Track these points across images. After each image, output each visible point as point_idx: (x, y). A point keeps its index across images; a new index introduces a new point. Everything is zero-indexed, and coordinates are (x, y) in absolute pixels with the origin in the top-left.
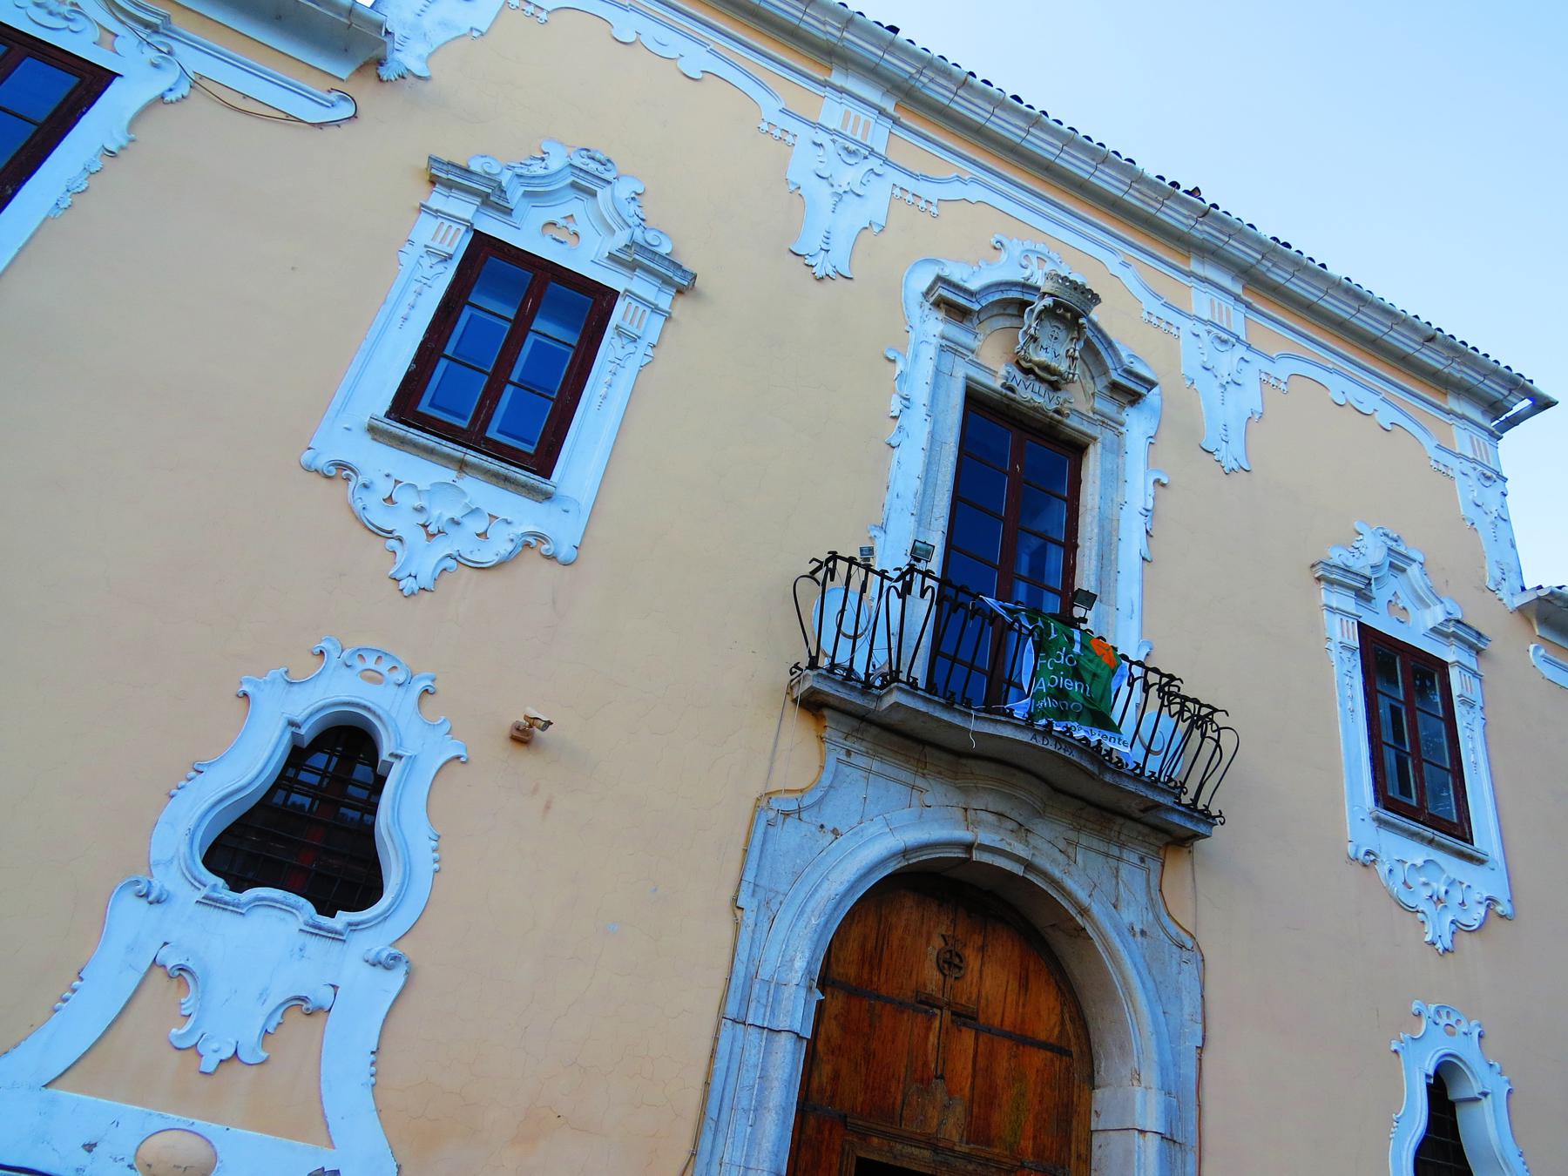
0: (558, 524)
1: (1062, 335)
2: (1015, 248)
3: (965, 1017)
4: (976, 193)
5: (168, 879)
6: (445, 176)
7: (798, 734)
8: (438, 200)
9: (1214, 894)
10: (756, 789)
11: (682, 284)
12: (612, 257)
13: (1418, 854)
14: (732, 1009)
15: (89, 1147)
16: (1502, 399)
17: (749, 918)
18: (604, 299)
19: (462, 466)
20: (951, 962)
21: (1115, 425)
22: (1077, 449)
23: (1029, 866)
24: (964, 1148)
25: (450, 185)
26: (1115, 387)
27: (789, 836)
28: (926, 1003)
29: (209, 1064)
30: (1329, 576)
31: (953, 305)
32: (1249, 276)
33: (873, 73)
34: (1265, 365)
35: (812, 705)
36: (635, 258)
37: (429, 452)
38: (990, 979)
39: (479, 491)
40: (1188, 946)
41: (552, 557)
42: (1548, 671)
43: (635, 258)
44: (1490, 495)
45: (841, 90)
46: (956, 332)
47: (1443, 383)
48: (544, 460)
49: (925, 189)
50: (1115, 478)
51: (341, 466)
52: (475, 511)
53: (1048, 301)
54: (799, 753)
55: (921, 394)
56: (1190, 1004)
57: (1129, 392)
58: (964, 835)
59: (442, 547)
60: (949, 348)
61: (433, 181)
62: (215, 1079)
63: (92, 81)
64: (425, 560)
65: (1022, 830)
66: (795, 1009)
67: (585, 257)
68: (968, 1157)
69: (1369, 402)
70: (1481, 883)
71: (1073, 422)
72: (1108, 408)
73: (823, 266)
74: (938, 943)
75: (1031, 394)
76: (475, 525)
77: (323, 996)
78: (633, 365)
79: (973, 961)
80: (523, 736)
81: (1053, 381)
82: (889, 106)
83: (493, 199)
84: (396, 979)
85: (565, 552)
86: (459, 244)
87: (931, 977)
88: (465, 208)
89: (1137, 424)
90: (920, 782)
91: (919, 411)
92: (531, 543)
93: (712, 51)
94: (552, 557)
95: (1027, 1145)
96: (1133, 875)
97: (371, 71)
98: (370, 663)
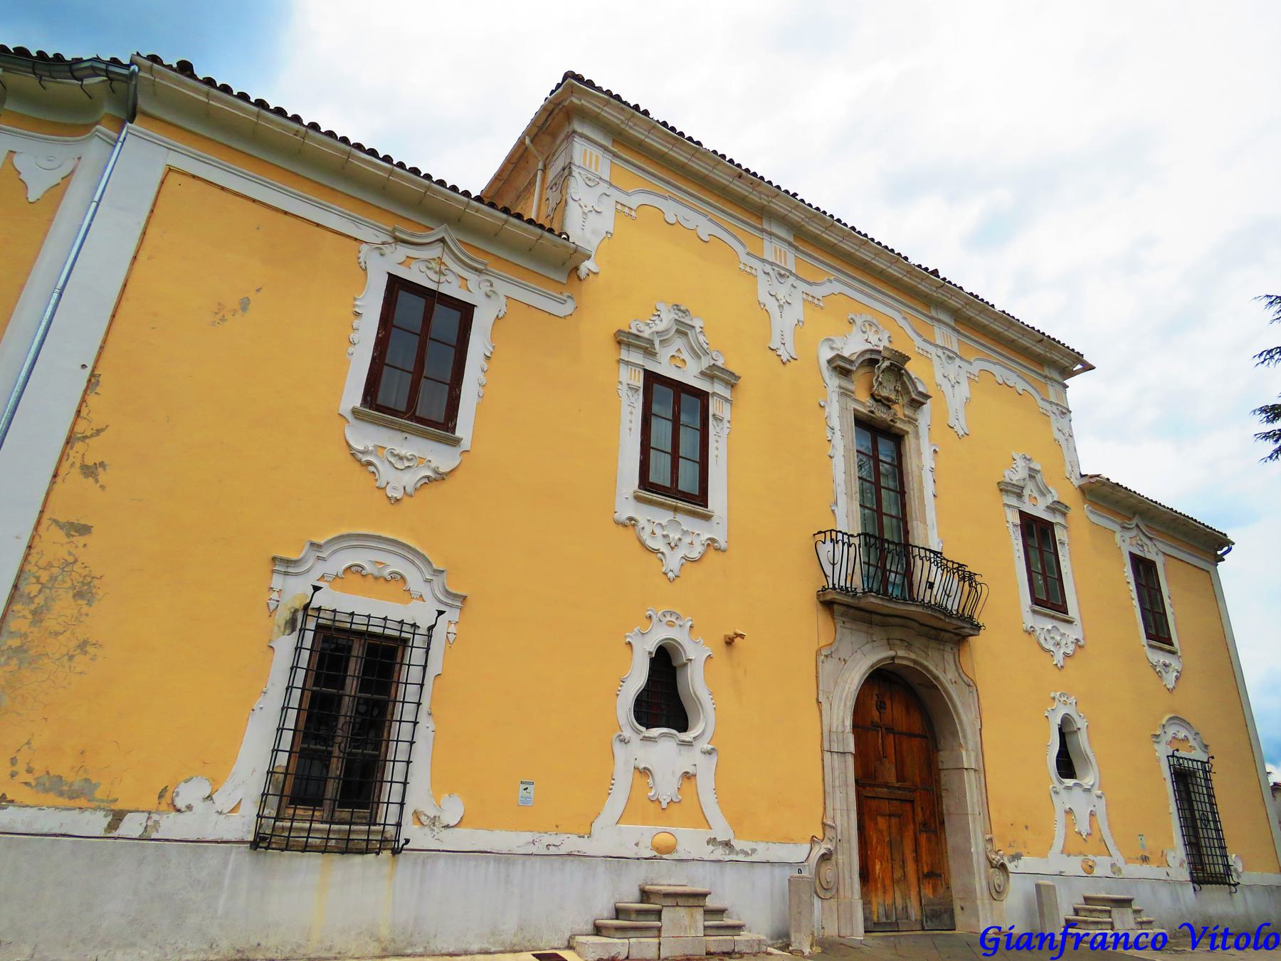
0: (717, 530)
1: (892, 379)
3: (890, 730)
5: (627, 733)
6: (625, 340)
8: (624, 355)
10: (816, 648)
12: (702, 373)
14: (826, 747)
15: (637, 845)
17: (825, 706)
18: (703, 396)
19: (676, 509)
21: (912, 421)
23: (915, 662)
24: (897, 785)
25: (629, 345)
26: (913, 400)
29: (664, 805)
30: (1006, 488)
31: (841, 368)
32: (957, 315)
33: (783, 221)
36: (712, 373)
37: (661, 505)
41: (717, 549)
42: (1094, 518)
43: (712, 373)
44: (1062, 423)
45: (771, 234)
46: (845, 383)
51: (631, 519)
52: (685, 532)
53: (887, 363)
58: (892, 653)
59: (681, 552)
61: (619, 343)
62: (662, 810)
63: (466, 311)
64: (673, 561)
65: (909, 647)
67: (689, 375)
68: (899, 788)
69: (1013, 379)
70: (1073, 633)
71: (899, 425)
72: (908, 412)
74: (875, 698)
75: (881, 414)
76: (687, 540)
77: (691, 770)
78: (724, 436)
81: (886, 403)
84: (714, 759)
85: (723, 545)
86: (639, 382)
88: (637, 357)
90: (871, 631)
93: (710, 220)
94: (717, 549)
95: (918, 779)
97: (574, 275)
98: (669, 618)
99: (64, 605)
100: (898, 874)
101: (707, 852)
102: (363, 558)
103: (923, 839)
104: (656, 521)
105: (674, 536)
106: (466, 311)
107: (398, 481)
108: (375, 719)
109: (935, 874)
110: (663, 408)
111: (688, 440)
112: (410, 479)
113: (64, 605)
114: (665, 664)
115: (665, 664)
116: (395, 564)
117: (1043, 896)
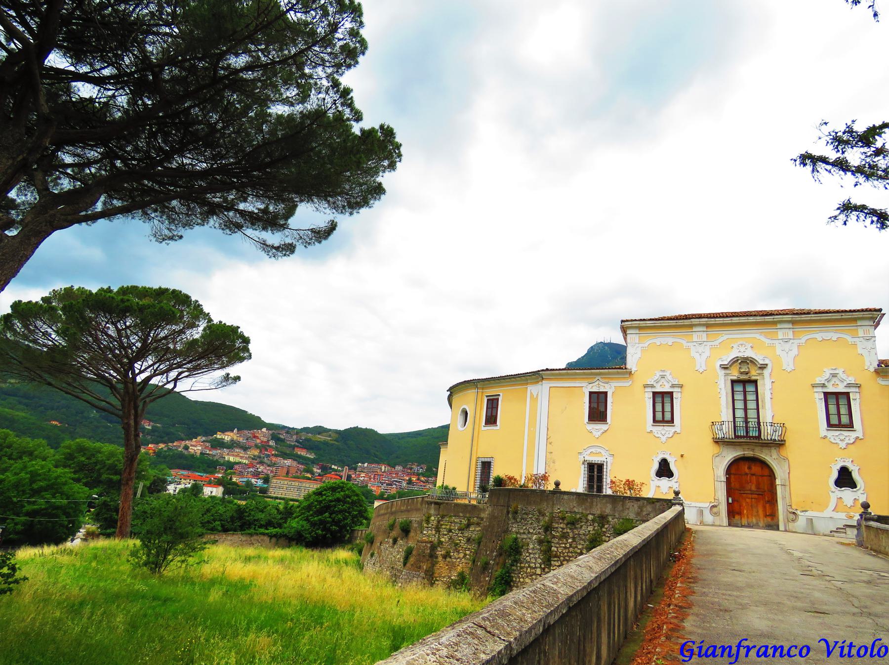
2: (735, 346)
4: (726, 337)
6: (645, 386)
9: (792, 449)
11: (681, 386)
13: (837, 433)
16: (874, 316)
20: (749, 468)
22: (755, 382)
27: (717, 459)
28: (747, 474)
34: (799, 341)
35: (716, 442)
38: (756, 469)
40: (786, 459)
42: (884, 383)
43: (673, 386)
44: (869, 344)
46: (728, 372)
49: (717, 343)
54: (715, 449)
57: (763, 367)
60: (726, 375)
63: (606, 393)
64: (664, 439)
65: (753, 450)
66: (724, 479)
70: (853, 435)
71: (754, 378)
79: (753, 468)
80: (682, 456)
83: (652, 386)
87: (747, 470)
89: (766, 372)
91: (723, 389)
92: (675, 432)
96: (774, 452)
99: (552, 465)
102: (593, 450)
103: (768, 505)
104: (659, 430)
106: (606, 393)
107: (597, 434)
108: (600, 479)
109: (772, 514)
110: (659, 400)
112: (599, 433)
113: (552, 465)
116: (599, 450)
117: (810, 521)
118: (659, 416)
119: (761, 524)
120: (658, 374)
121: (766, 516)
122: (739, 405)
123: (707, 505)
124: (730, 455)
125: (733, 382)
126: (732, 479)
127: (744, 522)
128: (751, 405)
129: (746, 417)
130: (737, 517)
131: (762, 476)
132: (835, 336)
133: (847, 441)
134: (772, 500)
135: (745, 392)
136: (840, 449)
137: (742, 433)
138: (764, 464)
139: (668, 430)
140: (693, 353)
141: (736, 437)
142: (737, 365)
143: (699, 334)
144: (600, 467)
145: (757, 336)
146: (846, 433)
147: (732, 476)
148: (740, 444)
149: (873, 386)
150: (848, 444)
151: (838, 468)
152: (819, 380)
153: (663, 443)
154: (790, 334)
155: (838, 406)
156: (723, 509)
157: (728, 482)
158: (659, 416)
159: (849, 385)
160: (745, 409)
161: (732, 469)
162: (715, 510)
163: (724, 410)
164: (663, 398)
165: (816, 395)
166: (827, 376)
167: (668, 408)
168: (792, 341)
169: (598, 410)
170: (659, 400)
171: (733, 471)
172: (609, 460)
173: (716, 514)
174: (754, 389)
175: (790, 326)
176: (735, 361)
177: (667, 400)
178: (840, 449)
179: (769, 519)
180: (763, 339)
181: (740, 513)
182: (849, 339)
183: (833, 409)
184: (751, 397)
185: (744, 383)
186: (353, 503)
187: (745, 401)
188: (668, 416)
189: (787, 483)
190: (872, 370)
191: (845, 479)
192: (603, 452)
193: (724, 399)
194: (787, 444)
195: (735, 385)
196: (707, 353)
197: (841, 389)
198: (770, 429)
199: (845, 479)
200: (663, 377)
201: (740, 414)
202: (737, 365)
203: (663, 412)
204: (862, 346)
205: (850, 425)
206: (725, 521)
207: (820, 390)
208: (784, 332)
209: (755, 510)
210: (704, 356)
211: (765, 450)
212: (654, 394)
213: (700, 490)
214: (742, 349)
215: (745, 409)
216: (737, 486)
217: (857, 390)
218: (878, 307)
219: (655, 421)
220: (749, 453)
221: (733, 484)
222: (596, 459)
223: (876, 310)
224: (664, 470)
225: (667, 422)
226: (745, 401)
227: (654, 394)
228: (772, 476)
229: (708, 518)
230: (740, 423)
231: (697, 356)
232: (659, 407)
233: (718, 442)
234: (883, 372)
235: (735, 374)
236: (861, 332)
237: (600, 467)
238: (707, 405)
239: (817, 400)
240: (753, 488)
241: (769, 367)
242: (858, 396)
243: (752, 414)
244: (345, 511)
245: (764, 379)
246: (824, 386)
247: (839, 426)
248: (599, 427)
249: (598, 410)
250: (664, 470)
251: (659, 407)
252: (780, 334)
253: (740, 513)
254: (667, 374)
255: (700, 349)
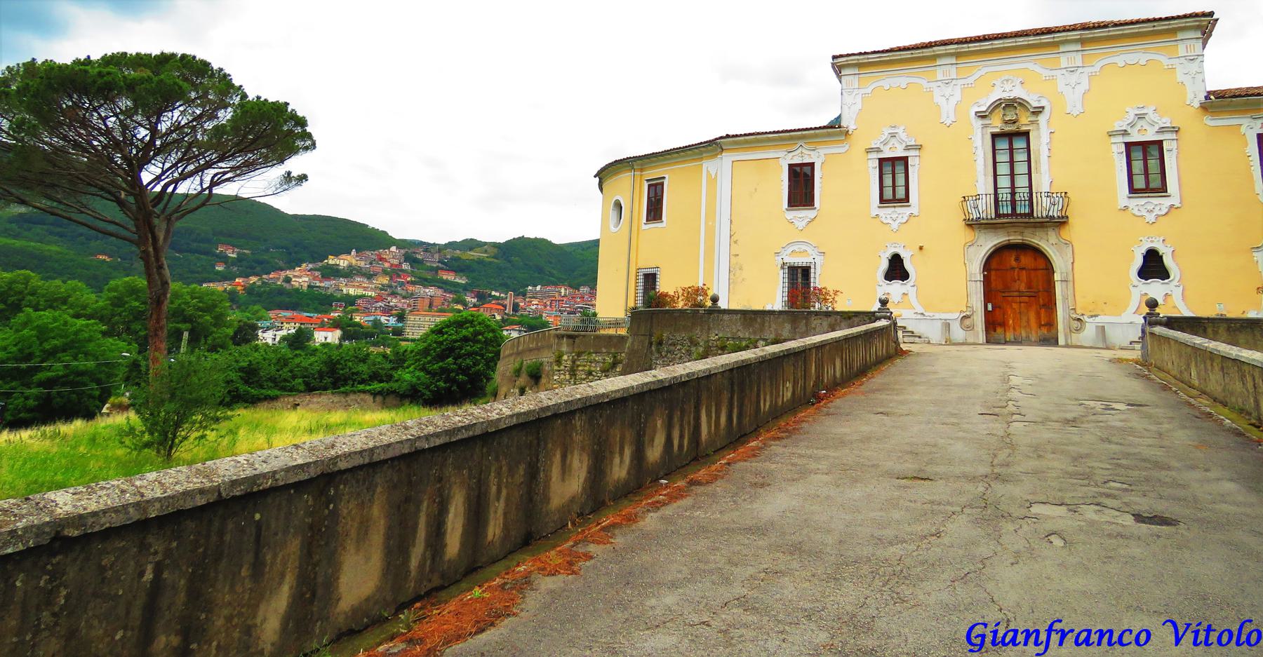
2: (998, 83)
4: (986, 70)
7: (968, 231)
9: (1076, 230)
11: (919, 148)
20: (1017, 259)
22: (1026, 134)
27: (971, 249)
28: (1013, 268)
31: (982, 116)
34: (1090, 69)
38: (1026, 260)
39: (899, 210)
40: (1068, 243)
43: (908, 148)
46: (986, 121)
47: (1173, 31)
48: (907, 199)
49: (970, 80)
50: (1039, 137)
55: (978, 143)
56: (1070, 254)
60: (985, 126)
64: (895, 225)
70: (1166, 202)
71: (1024, 128)
73: (948, 122)
75: (1008, 128)
80: (921, 248)
82: (954, 61)
87: (1014, 263)
89: (1042, 119)
91: (980, 148)
100: (1024, 323)
101: (914, 316)
105: (894, 216)
110: (887, 169)
111: (900, 180)
114: (896, 261)
115: (896, 261)
118: (888, 194)
119: (1034, 337)
120: (887, 131)
121: (1040, 326)
122: (1003, 169)
123: (956, 315)
124: (989, 242)
125: (994, 136)
126: (993, 278)
127: (1010, 336)
128: (1021, 168)
129: (1013, 187)
130: (999, 330)
131: (1036, 270)
132: (1142, 58)
133: (1157, 212)
134: (1050, 304)
135: (1011, 150)
136: (1147, 223)
137: (1006, 209)
138: (1038, 252)
139: (901, 212)
140: (938, 98)
141: (998, 215)
142: (1000, 112)
143: (945, 69)
144: (806, 271)
145: (1030, 66)
146: (1155, 201)
147: (993, 273)
148: (1002, 226)
149: (1198, 127)
150: (1158, 216)
151: (1144, 251)
152: (1117, 126)
153: (896, 231)
154: (1078, 59)
155: (1146, 163)
156: (979, 320)
157: (987, 281)
158: (888, 194)
159: (1162, 130)
160: (1012, 175)
161: (992, 263)
162: (967, 322)
163: (981, 178)
164: (893, 167)
165: (1114, 148)
166: (1131, 117)
167: (900, 180)
168: (1080, 70)
169: (801, 187)
170: (887, 169)
171: (994, 265)
172: (819, 260)
173: (970, 328)
174: (1025, 145)
175: (1079, 47)
176: (997, 105)
177: (900, 169)
178: (1147, 223)
179: (1044, 331)
180: (1037, 68)
181: (1004, 325)
182: (1164, 61)
183: (1138, 166)
184: (1020, 157)
185: (1010, 136)
186: (487, 342)
187: (1012, 162)
188: (901, 193)
189: (1070, 278)
190: (1197, 105)
191: (1153, 266)
192: (810, 251)
193: (980, 161)
194: (1070, 220)
195: (997, 140)
196: (957, 97)
197: (1150, 136)
198: (1046, 202)
199: (1153, 266)
200: (893, 136)
201: (1004, 182)
202: (1000, 112)
203: (894, 186)
204: (1182, 71)
205: (1162, 189)
206: (982, 337)
207: (1120, 139)
208: (1069, 57)
209: (1024, 319)
210: (953, 101)
211: (1040, 233)
212: (881, 161)
213: (942, 295)
214: (1008, 87)
215: (1012, 175)
216: (1000, 287)
217: (1174, 136)
218: (1208, 10)
219: (882, 200)
220: (1016, 238)
221: (993, 285)
222: (800, 261)
223: (1204, 15)
224: (896, 270)
225: (900, 201)
226: (1012, 162)
227: (881, 161)
228: (1049, 269)
229: (958, 333)
230: (1005, 195)
231: (942, 101)
232: (888, 181)
233: (974, 224)
234: (1212, 107)
235: (997, 124)
236: (1181, 49)
237: (806, 271)
238: (959, 172)
239: (1115, 155)
240: (1023, 287)
241: (1047, 110)
242: (1174, 143)
243: (1021, 182)
244: (476, 354)
245: (1038, 129)
246: (1125, 133)
247: (1148, 190)
248: (804, 214)
249: (801, 187)
250: (896, 270)
251: (888, 181)
252: (1064, 61)
253: (1004, 325)
254: (900, 131)
255: (948, 91)
